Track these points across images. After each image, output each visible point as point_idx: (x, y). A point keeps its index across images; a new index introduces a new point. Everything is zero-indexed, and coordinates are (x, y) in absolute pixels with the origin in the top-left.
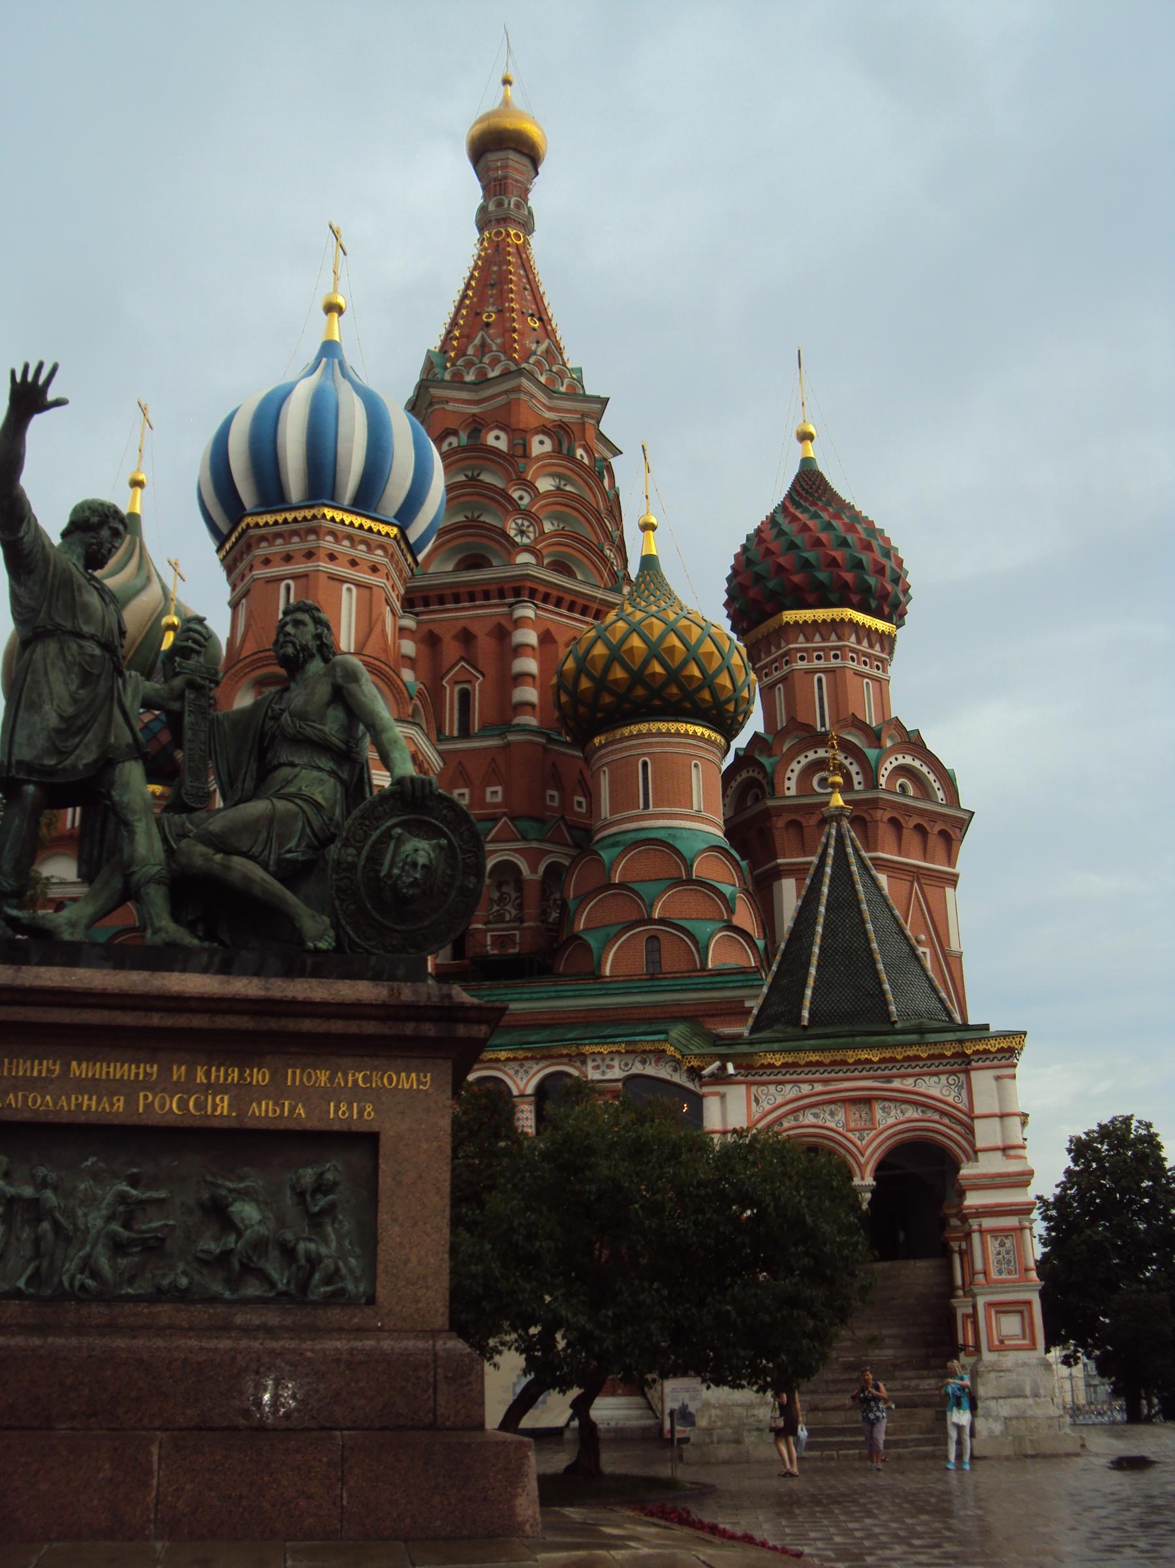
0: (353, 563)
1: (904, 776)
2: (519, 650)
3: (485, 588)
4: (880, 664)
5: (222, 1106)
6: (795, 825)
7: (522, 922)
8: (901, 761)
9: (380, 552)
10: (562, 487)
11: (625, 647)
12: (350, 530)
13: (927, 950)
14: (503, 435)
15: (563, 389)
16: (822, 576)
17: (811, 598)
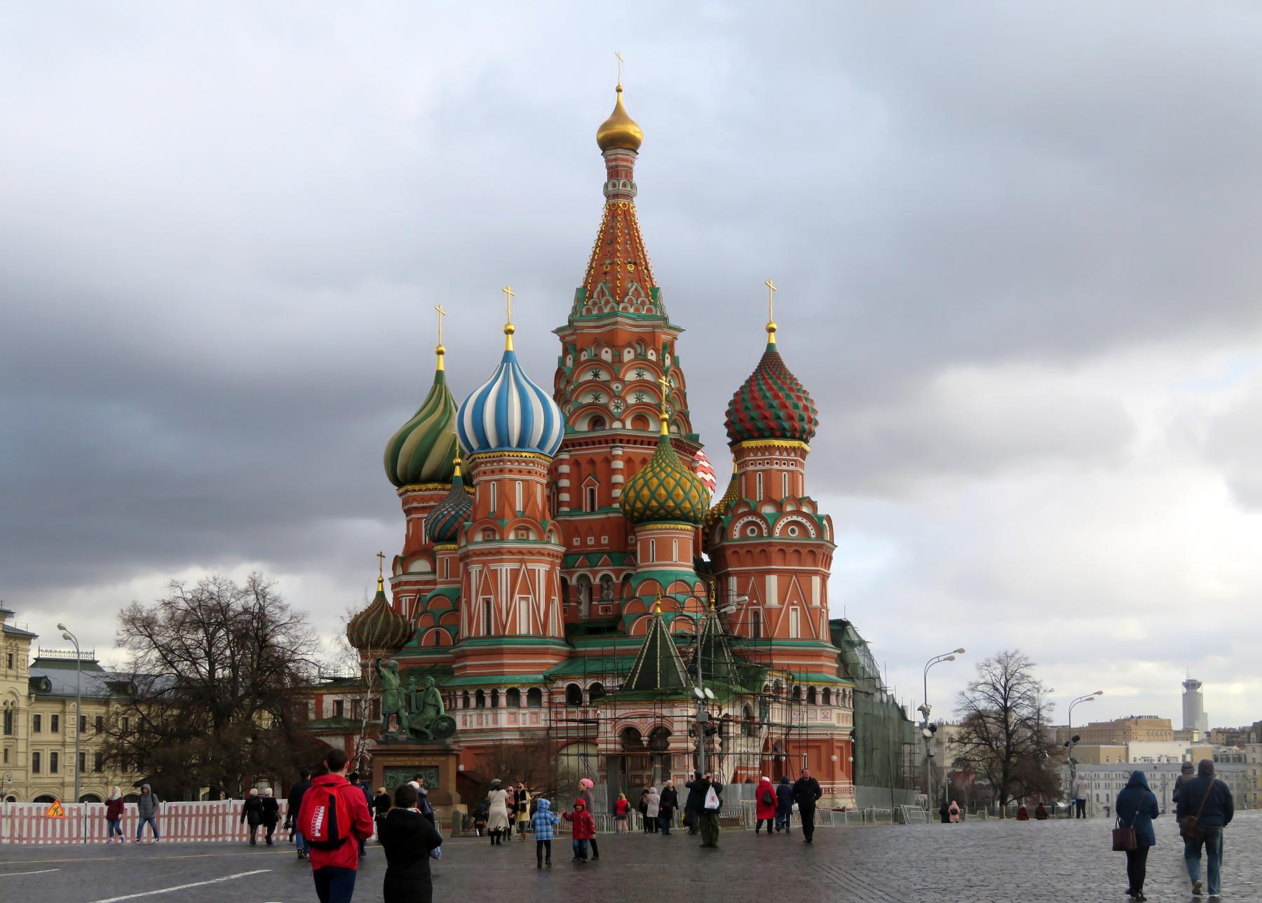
0: (520, 471)
1: (793, 525)
2: (614, 471)
3: (599, 439)
4: (794, 463)
5: (417, 763)
6: (735, 552)
7: (613, 601)
8: (790, 519)
9: (531, 464)
10: (641, 374)
11: (641, 494)
12: (517, 458)
13: (798, 608)
14: (609, 350)
15: (644, 312)
16: (760, 424)
17: (755, 434)
